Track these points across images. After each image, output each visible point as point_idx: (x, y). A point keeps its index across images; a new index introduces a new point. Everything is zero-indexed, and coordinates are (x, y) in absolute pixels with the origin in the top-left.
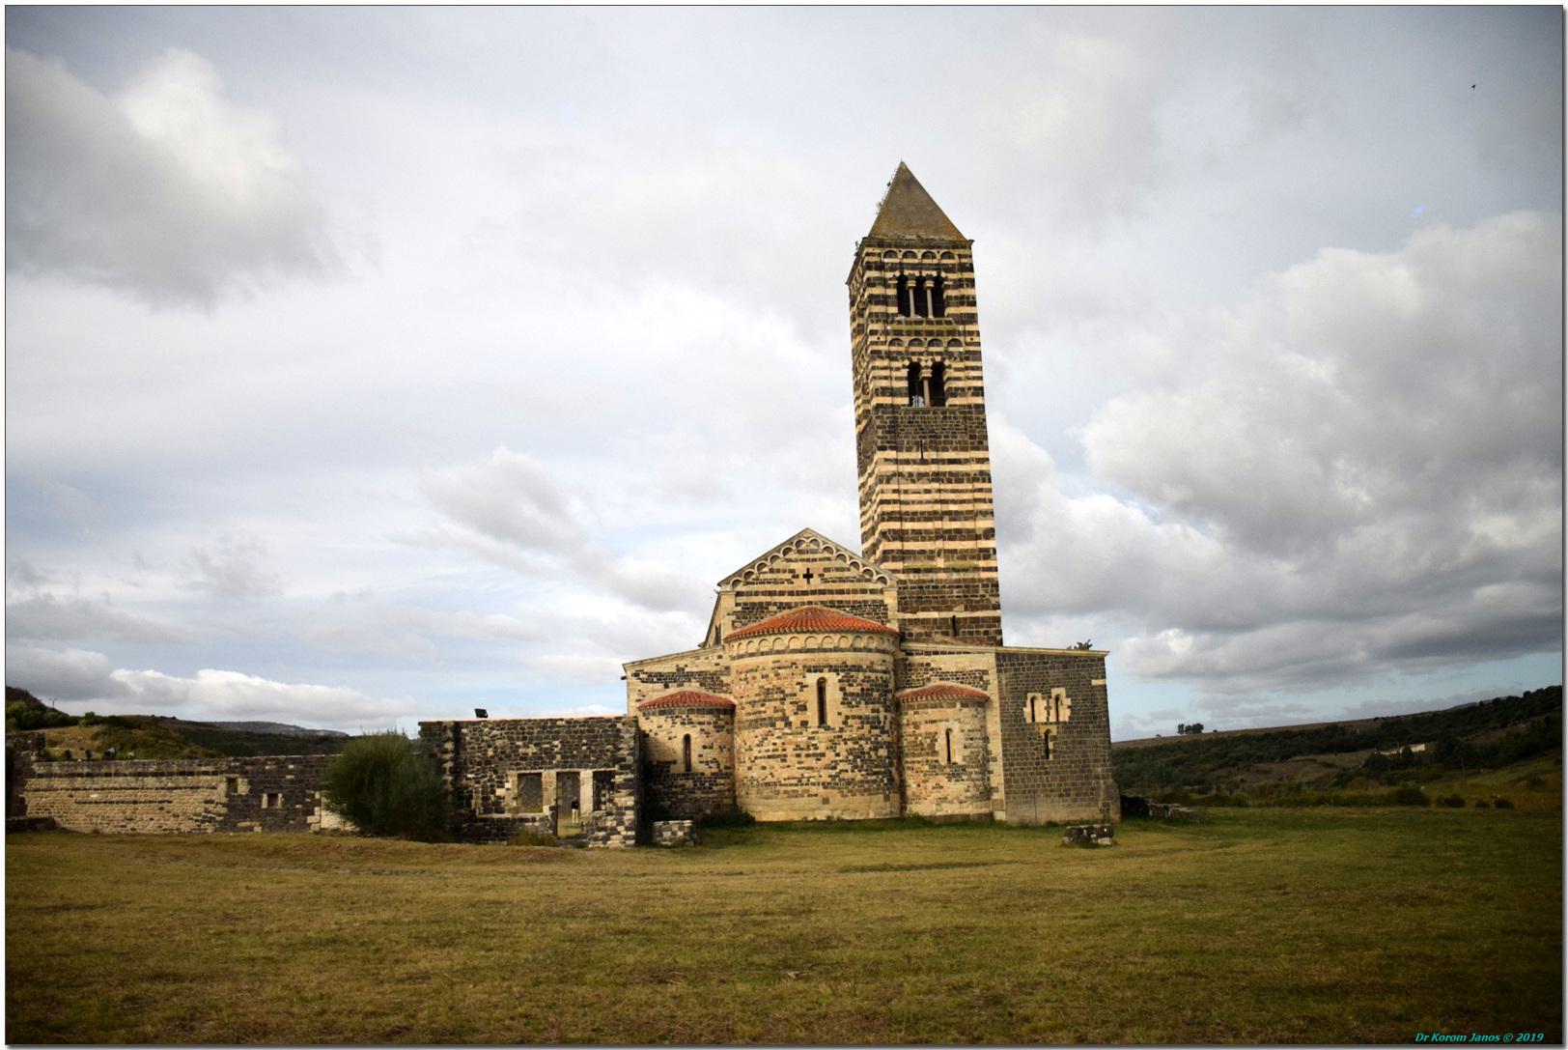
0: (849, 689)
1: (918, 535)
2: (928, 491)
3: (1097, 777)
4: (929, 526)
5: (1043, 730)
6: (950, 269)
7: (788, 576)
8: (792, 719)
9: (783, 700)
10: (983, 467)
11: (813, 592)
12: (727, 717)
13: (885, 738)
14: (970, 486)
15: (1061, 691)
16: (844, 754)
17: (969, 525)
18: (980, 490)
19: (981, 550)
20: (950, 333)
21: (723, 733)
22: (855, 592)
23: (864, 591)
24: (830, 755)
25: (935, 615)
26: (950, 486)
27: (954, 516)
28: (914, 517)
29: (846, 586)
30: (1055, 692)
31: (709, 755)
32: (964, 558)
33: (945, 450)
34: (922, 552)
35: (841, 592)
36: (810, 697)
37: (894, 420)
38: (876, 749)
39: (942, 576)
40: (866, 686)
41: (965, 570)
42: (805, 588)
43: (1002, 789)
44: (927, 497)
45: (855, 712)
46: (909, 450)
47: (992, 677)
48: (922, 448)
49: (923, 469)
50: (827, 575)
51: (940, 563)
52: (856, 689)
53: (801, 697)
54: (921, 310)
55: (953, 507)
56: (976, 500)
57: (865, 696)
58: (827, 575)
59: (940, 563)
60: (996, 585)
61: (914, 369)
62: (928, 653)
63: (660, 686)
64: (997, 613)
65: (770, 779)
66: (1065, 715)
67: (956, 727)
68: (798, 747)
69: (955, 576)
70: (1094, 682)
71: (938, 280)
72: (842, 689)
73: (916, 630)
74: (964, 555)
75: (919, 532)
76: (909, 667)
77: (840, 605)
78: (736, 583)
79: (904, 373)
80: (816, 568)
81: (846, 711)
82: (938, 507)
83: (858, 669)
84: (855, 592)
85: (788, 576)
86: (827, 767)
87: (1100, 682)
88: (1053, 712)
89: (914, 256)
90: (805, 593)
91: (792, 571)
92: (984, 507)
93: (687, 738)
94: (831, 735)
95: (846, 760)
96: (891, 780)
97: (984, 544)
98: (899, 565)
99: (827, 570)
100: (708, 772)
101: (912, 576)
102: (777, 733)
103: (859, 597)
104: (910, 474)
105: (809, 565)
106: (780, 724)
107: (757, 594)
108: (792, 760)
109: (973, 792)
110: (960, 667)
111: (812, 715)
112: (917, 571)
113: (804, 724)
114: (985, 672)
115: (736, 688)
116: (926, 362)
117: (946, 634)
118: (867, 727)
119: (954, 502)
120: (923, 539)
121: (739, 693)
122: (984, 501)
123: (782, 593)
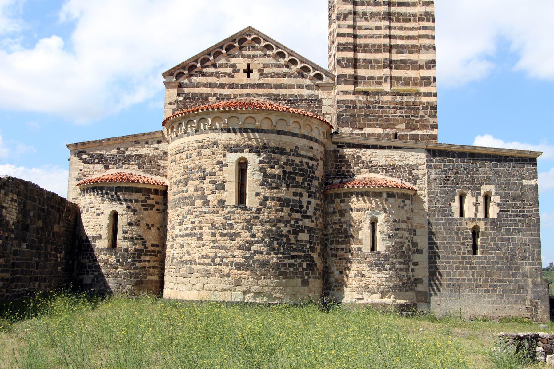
0: (269, 170)
1: (369, 64)
2: (379, 28)
3: (525, 275)
4: (379, 56)
5: (471, 225)
7: (229, 70)
8: (209, 198)
9: (203, 179)
10: (428, 9)
11: (252, 86)
12: (159, 198)
14: (416, 25)
15: (491, 188)
16: (260, 234)
17: (413, 57)
18: (425, 28)
19: (423, 78)
21: (152, 212)
22: (291, 87)
23: (300, 87)
24: (245, 235)
25: (380, 131)
26: (398, 25)
27: (401, 49)
28: (366, 48)
30: (484, 189)
31: (135, 231)
32: (408, 84)
34: (372, 78)
36: (230, 175)
38: (295, 233)
39: (388, 98)
40: (288, 169)
41: (408, 94)
42: (246, 81)
43: (426, 280)
45: (275, 193)
47: (422, 171)
49: (376, 9)
50: (266, 71)
51: (386, 87)
52: (277, 171)
53: (220, 176)
55: (400, 42)
56: (420, 36)
57: (287, 178)
58: (266, 71)
60: (435, 108)
63: (100, 166)
64: (435, 132)
65: (187, 258)
66: (493, 212)
67: (381, 218)
68: (214, 226)
69: (398, 99)
70: (524, 182)
72: (262, 170)
74: (407, 82)
75: (370, 61)
77: (277, 98)
78: (180, 75)
80: (257, 63)
81: (266, 192)
82: (387, 41)
83: (282, 151)
84: (291, 87)
85: (229, 70)
87: (532, 182)
88: (481, 208)
90: (243, 86)
91: (234, 66)
92: (427, 42)
93: (115, 216)
94: (246, 215)
95: (262, 242)
96: (312, 265)
97: (425, 73)
98: (351, 88)
99: (265, 66)
100: (132, 249)
101: (361, 97)
102: (196, 212)
103: (295, 92)
104: (364, 14)
105: (249, 61)
106: (199, 203)
107: (198, 86)
108: (207, 238)
109: (396, 281)
110: (390, 161)
111: (230, 195)
112: (365, 93)
113: (221, 203)
115: (169, 172)
118: (287, 210)
119: (401, 37)
120: (373, 68)
121: (172, 176)
122: (427, 37)
123: (222, 86)
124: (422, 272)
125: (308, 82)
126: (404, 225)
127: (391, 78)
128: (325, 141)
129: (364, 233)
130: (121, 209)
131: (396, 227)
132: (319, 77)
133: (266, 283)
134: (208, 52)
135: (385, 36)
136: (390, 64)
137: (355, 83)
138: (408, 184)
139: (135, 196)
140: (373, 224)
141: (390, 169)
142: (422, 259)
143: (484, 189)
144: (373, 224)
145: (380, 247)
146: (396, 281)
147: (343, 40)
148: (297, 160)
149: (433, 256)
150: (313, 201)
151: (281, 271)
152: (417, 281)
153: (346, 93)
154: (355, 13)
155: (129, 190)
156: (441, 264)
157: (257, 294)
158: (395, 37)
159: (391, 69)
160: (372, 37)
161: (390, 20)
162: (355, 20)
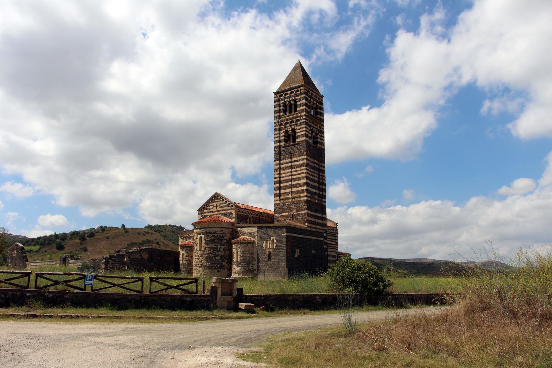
1: (285, 188)
2: (288, 173)
6: (298, 96)
11: (217, 211)
13: (220, 253)
15: (273, 238)
17: (299, 182)
20: (296, 117)
23: (228, 210)
24: (201, 258)
25: (287, 214)
29: (225, 208)
30: (272, 238)
31: (188, 259)
32: (297, 193)
33: (294, 158)
34: (286, 193)
35: (223, 210)
36: (198, 241)
37: (280, 151)
38: (215, 257)
40: (212, 238)
44: (288, 174)
46: (283, 160)
47: (256, 234)
48: (287, 158)
51: (290, 196)
52: (209, 239)
54: (290, 112)
55: (295, 177)
57: (212, 241)
59: (290, 196)
61: (286, 132)
62: (241, 227)
67: (239, 250)
71: (295, 101)
73: (282, 219)
75: (285, 186)
76: (237, 232)
78: (201, 210)
79: (283, 134)
81: (206, 246)
82: (290, 177)
83: (211, 233)
84: (226, 210)
86: (200, 262)
89: (288, 94)
90: (215, 211)
96: (222, 266)
98: (278, 198)
103: (227, 211)
109: (243, 270)
111: (198, 248)
112: (283, 199)
114: (254, 232)
116: (289, 129)
117: (290, 220)
118: (212, 250)
119: (295, 175)
124: (255, 267)
125: (230, 208)
126: (247, 252)
127: (292, 192)
128: (231, 227)
129: (235, 256)
130: (184, 252)
131: (243, 253)
132: (232, 206)
133: (206, 272)
134: (207, 202)
135: (289, 176)
136: (292, 186)
137: (280, 196)
138: (253, 239)
139: (187, 248)
140: (237, 252)
141: (249, 234)
142: (255, 263)
143: (272, 238)
144: (237, 252)
145: (239, 260)
146: (243, 270)
147: (276, 180)
148: (216, 235)
149: (258, 262)
150: (223, 247)
151: (210, 268)
152: (255, 270)
153: (277, 200)
154: (280, 168)
155: (186, 247)
156: (260, 264)
157: (204, 275)
158: (293, 175)
159: (292, 188)
160: (286, 177)
161: (291, 168)
162: (280, 171)
